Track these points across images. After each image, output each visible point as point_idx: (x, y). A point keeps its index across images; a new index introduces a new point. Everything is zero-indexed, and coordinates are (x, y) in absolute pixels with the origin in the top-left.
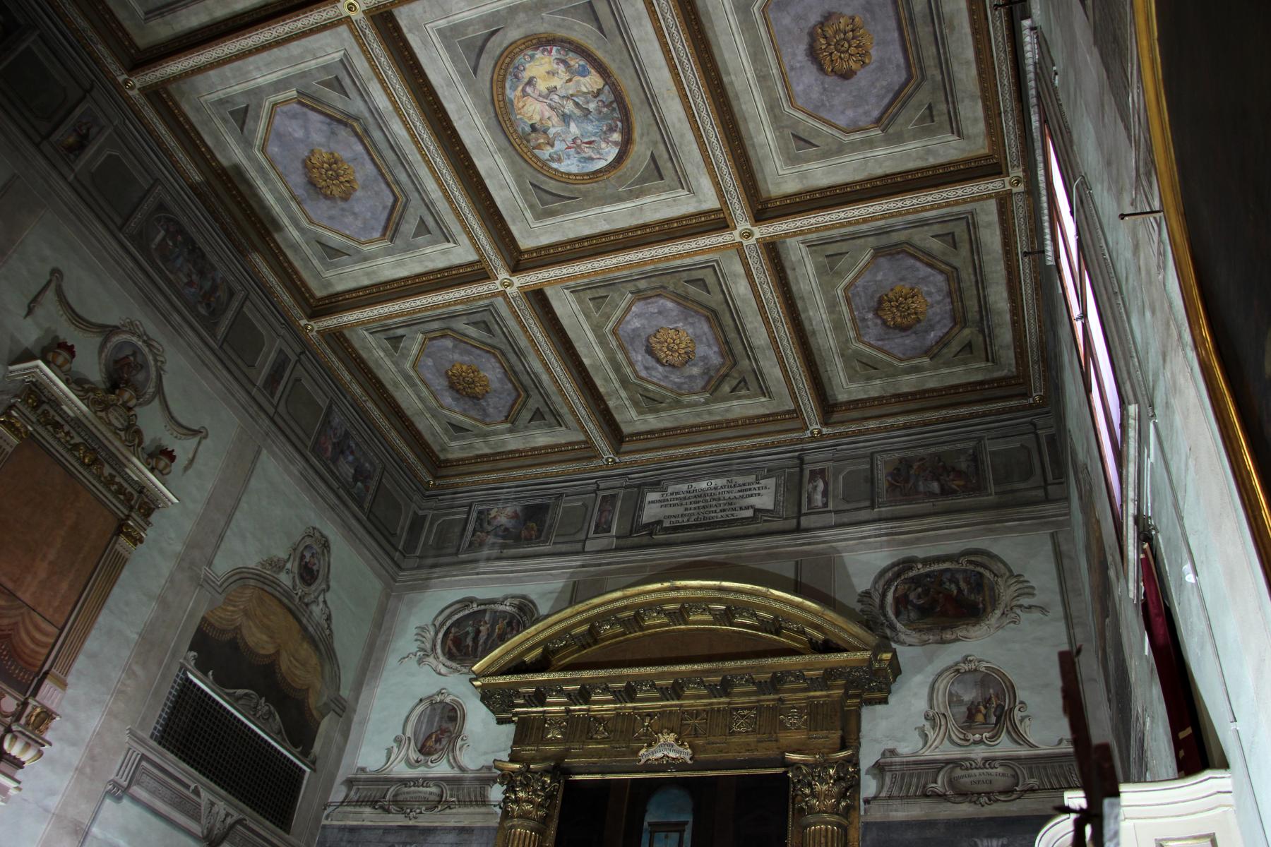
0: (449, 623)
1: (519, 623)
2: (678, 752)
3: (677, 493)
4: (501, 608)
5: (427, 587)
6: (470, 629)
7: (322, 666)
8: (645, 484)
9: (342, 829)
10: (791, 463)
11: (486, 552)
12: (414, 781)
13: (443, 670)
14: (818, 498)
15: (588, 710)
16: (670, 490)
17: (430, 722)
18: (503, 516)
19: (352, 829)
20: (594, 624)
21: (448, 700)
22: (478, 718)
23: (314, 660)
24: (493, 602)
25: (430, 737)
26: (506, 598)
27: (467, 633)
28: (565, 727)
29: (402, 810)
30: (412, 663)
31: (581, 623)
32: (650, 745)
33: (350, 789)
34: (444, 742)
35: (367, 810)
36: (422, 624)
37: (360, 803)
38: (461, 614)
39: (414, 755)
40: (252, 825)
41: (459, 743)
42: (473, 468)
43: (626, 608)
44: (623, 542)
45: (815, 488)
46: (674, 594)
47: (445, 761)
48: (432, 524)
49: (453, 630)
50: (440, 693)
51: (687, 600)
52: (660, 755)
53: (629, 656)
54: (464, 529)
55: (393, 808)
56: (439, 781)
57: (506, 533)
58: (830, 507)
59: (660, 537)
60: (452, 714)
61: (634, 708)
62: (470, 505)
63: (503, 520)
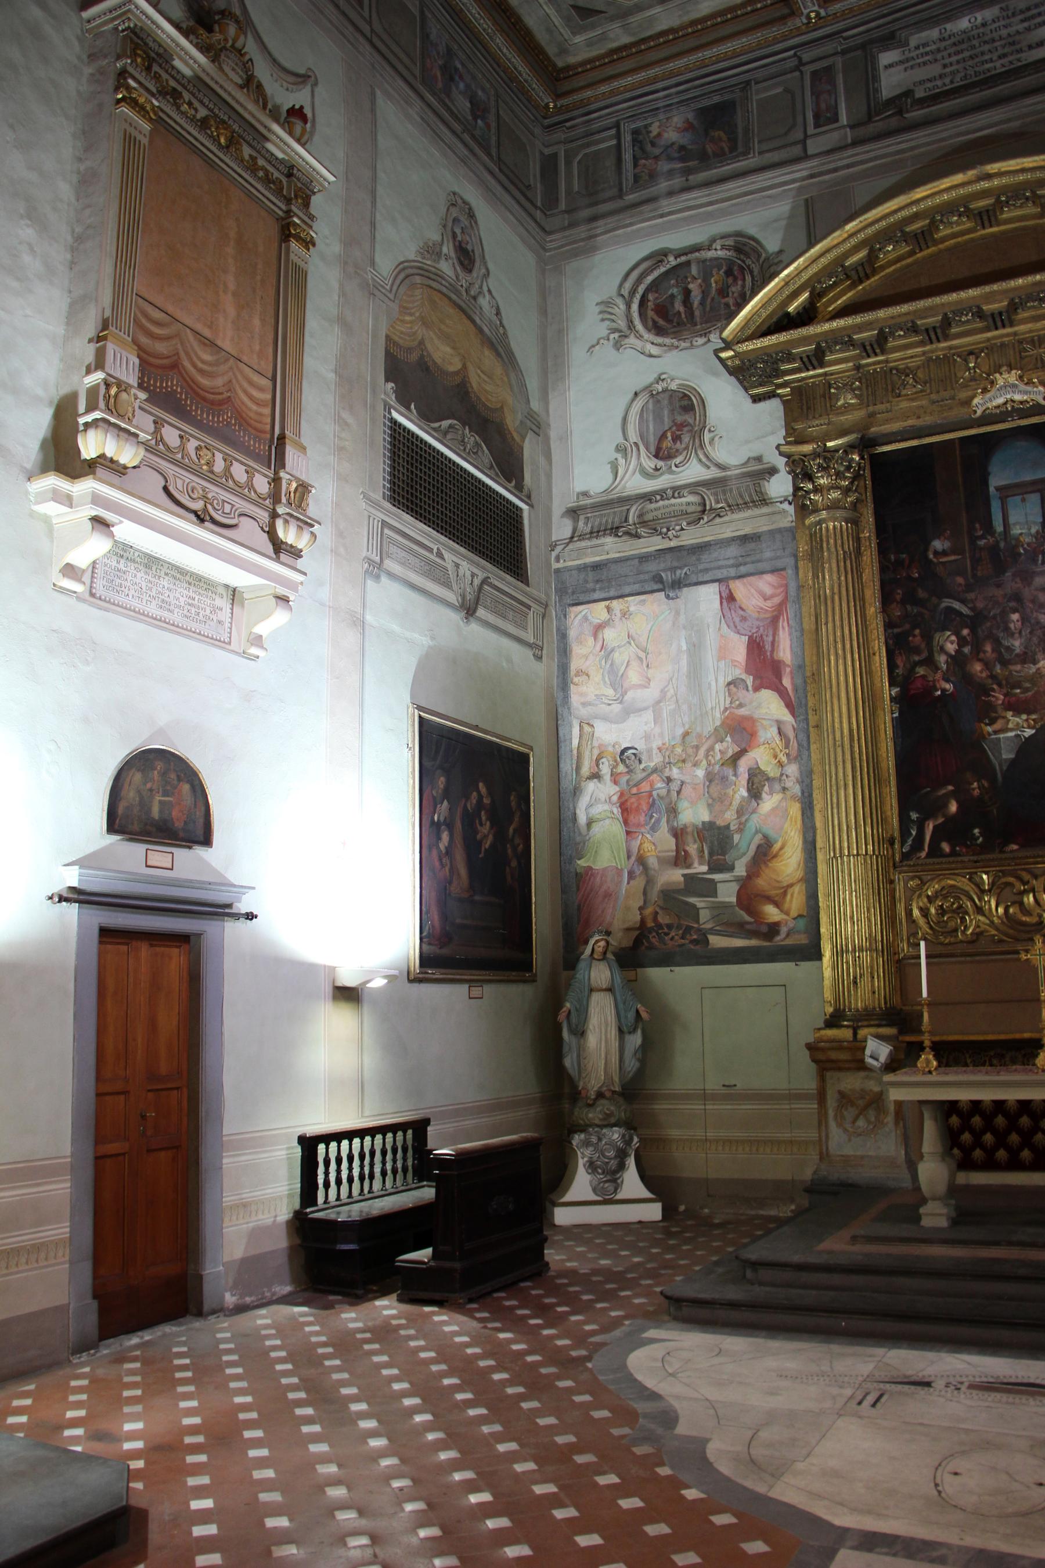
0: (641, 289)
1: (741, 269)
2: (1026, 393)
3: (925, 45)
4: (711, 254)
5: (594, 249)
6: (675, 291)
7: (508, 375)
8: (872, 41)
9: (583, 568)
11: (663, 185)
12: (662, 494)
13: (654, 350)
15: (887, 361)
16: (913, 42)
17: (658, 417)
18: (672, 129)
19: (596, 567)
20: (873, 244)
21: (673, 386)
22: (724, 400)
23: (499, 370)
24: (697, 248)
25: (663, 436)
26: (713, 240)
27: (672, 296)
28: (859, 388)
29: (655, 531)
30: (607, 350)
31: (856, 249)
32: (985, 391)
33: (576, 520)
34: (686, 438)
35: (609, 540)
36: (604, 298)
37: (595, 533)
38: (656, 274)
39: (649, 463)
40: (496, 583)
41: (707, 436)
42: (610, 71)
43: (916, 217)
44: (862, 132)
46: (985, 185)
47: (694, 461)
48: (568, 163)
49: (651, 297)
50: (659, 379)
51: (1003, 190)
52: (1001, 401)
53: (924, 282)
54: (619, 160)
55: (641, 531)
56: (694, 487)
57: (683, 153)
59: (916, 114)
60: (685, 402)
61: (950, 348)
62: (617, 125)
63: (672, 135)
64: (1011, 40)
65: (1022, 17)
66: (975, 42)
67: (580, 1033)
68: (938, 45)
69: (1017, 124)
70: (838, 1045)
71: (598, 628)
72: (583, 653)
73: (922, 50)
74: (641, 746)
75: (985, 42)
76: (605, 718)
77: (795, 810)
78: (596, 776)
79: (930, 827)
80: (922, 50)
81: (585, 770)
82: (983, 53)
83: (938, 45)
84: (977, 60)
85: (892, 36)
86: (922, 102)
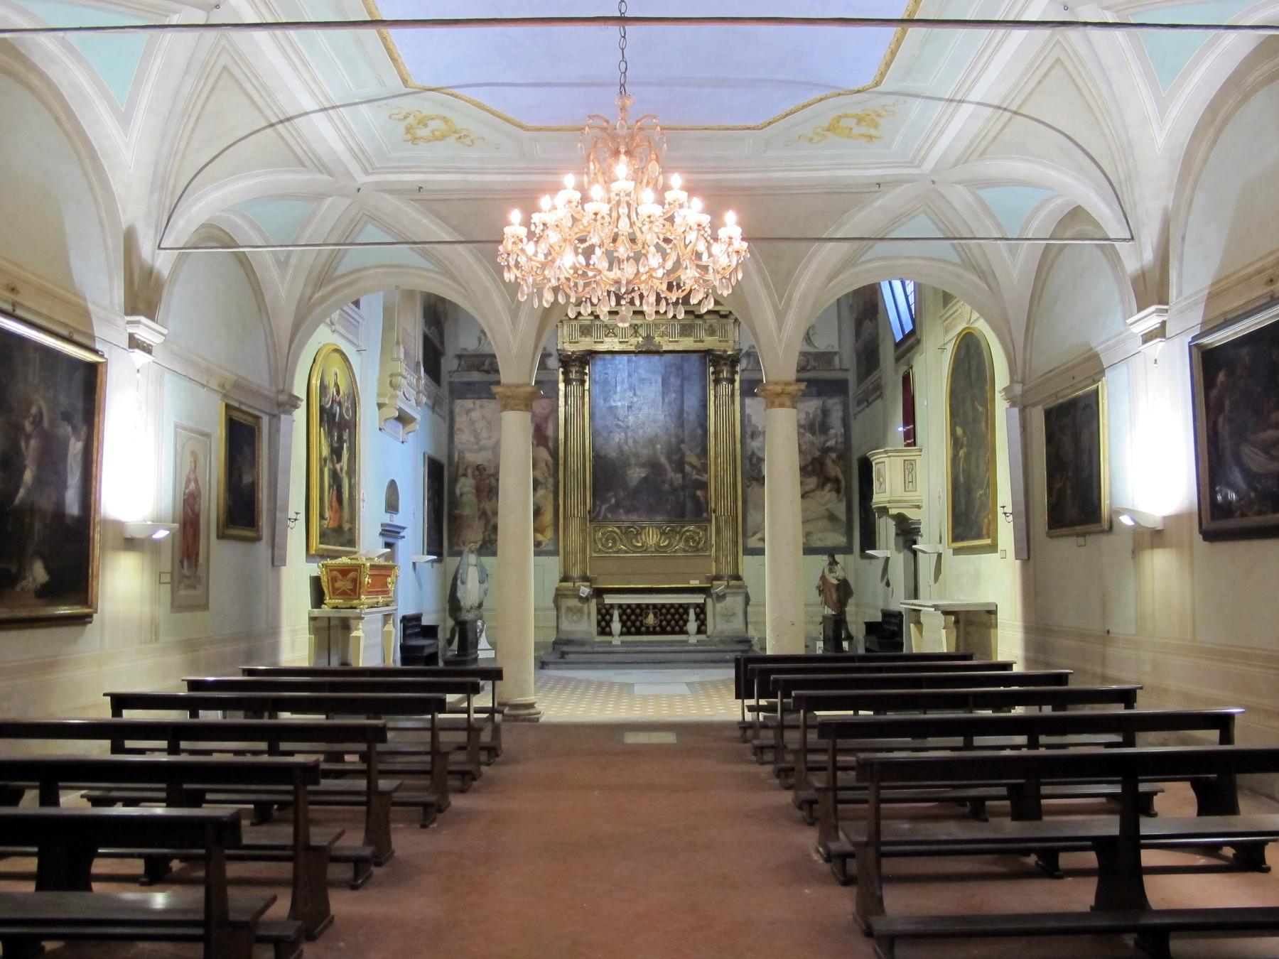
67: (463, 583)
70: (567, 589)
71: (468, 412)
72: (461, 421)
74: (486, 464)
76: (471, 451)
77: (551, 496)
78: (465, 475)
79: (604, 508)
81: (461, 471)
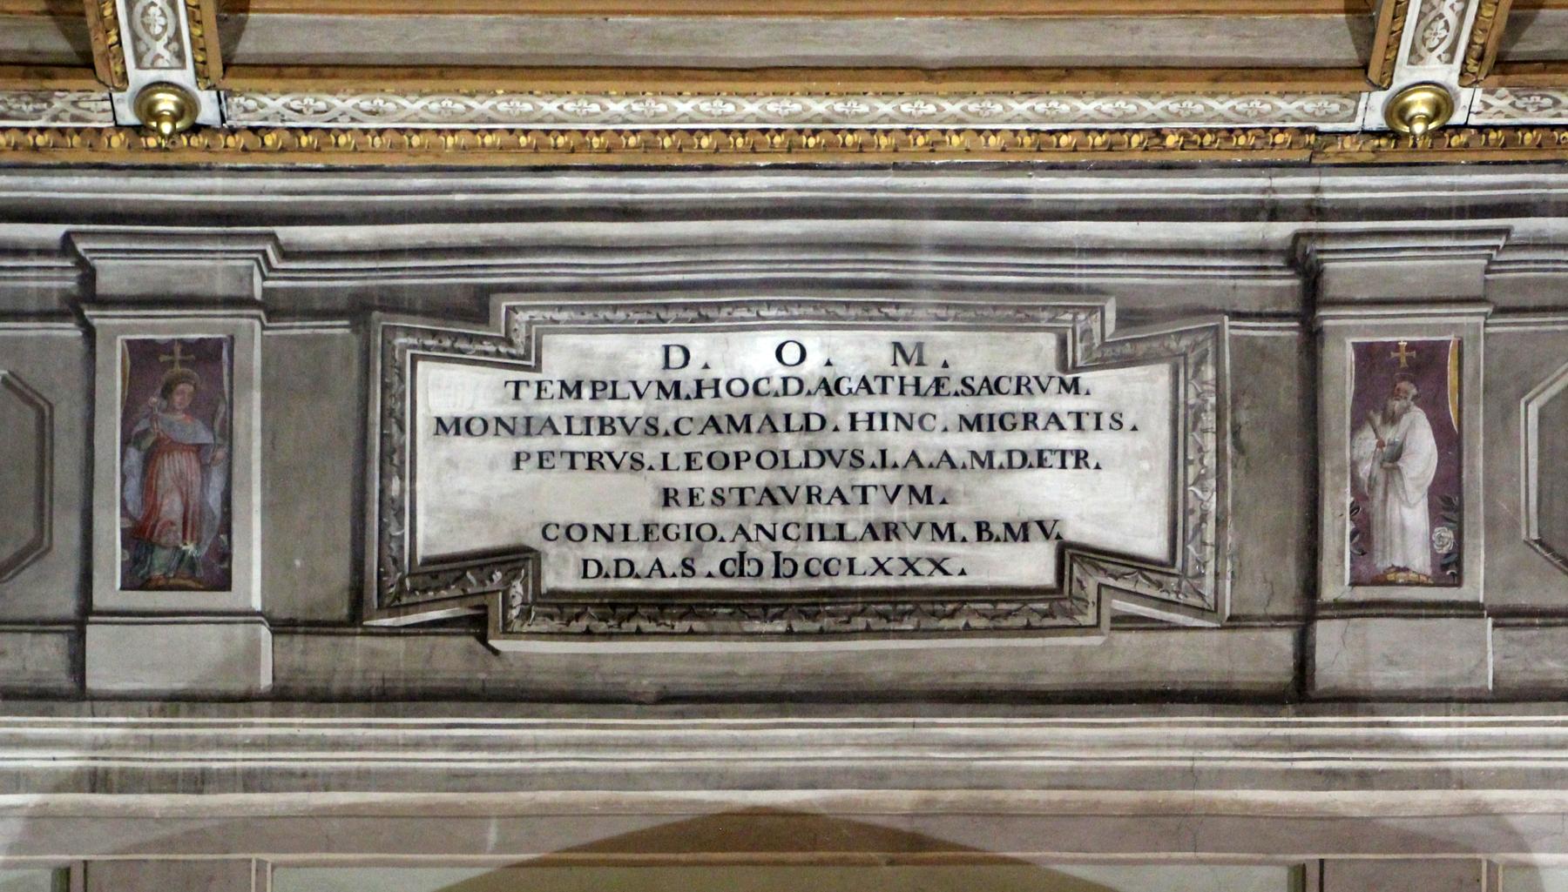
10: (1253, 289)
14: (1410, 528)
45: (1393, 456)
58: (1474, 588)
64: (920, 480)
65: (967, 406)
66: (786, 441)
68: (651, 405)
69: (906, 798)
73: (584, 406)
75: (826, 456)
80: (584, 406)
82: (813, 496)
83: (651, 405)
84: (787, 514)
85: (473, 308)
86: (566, 610)
